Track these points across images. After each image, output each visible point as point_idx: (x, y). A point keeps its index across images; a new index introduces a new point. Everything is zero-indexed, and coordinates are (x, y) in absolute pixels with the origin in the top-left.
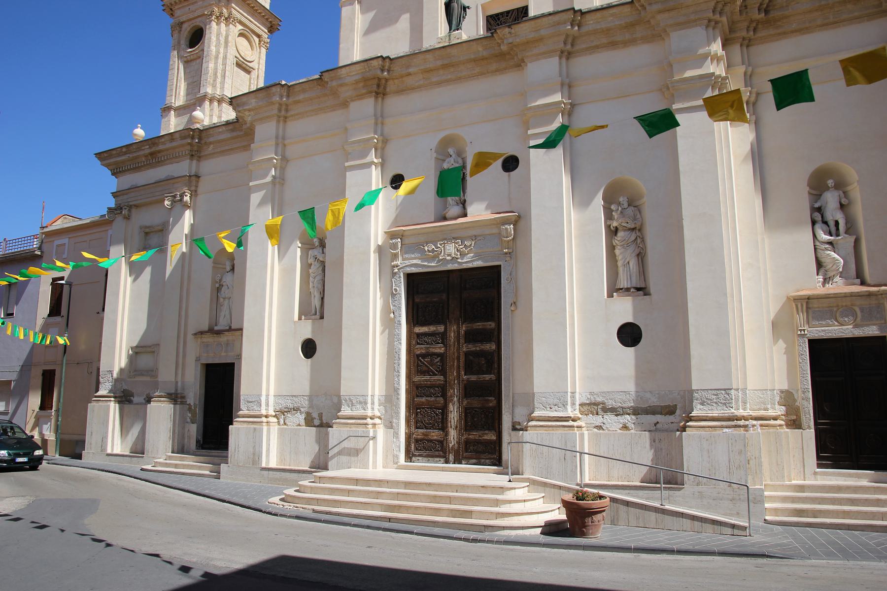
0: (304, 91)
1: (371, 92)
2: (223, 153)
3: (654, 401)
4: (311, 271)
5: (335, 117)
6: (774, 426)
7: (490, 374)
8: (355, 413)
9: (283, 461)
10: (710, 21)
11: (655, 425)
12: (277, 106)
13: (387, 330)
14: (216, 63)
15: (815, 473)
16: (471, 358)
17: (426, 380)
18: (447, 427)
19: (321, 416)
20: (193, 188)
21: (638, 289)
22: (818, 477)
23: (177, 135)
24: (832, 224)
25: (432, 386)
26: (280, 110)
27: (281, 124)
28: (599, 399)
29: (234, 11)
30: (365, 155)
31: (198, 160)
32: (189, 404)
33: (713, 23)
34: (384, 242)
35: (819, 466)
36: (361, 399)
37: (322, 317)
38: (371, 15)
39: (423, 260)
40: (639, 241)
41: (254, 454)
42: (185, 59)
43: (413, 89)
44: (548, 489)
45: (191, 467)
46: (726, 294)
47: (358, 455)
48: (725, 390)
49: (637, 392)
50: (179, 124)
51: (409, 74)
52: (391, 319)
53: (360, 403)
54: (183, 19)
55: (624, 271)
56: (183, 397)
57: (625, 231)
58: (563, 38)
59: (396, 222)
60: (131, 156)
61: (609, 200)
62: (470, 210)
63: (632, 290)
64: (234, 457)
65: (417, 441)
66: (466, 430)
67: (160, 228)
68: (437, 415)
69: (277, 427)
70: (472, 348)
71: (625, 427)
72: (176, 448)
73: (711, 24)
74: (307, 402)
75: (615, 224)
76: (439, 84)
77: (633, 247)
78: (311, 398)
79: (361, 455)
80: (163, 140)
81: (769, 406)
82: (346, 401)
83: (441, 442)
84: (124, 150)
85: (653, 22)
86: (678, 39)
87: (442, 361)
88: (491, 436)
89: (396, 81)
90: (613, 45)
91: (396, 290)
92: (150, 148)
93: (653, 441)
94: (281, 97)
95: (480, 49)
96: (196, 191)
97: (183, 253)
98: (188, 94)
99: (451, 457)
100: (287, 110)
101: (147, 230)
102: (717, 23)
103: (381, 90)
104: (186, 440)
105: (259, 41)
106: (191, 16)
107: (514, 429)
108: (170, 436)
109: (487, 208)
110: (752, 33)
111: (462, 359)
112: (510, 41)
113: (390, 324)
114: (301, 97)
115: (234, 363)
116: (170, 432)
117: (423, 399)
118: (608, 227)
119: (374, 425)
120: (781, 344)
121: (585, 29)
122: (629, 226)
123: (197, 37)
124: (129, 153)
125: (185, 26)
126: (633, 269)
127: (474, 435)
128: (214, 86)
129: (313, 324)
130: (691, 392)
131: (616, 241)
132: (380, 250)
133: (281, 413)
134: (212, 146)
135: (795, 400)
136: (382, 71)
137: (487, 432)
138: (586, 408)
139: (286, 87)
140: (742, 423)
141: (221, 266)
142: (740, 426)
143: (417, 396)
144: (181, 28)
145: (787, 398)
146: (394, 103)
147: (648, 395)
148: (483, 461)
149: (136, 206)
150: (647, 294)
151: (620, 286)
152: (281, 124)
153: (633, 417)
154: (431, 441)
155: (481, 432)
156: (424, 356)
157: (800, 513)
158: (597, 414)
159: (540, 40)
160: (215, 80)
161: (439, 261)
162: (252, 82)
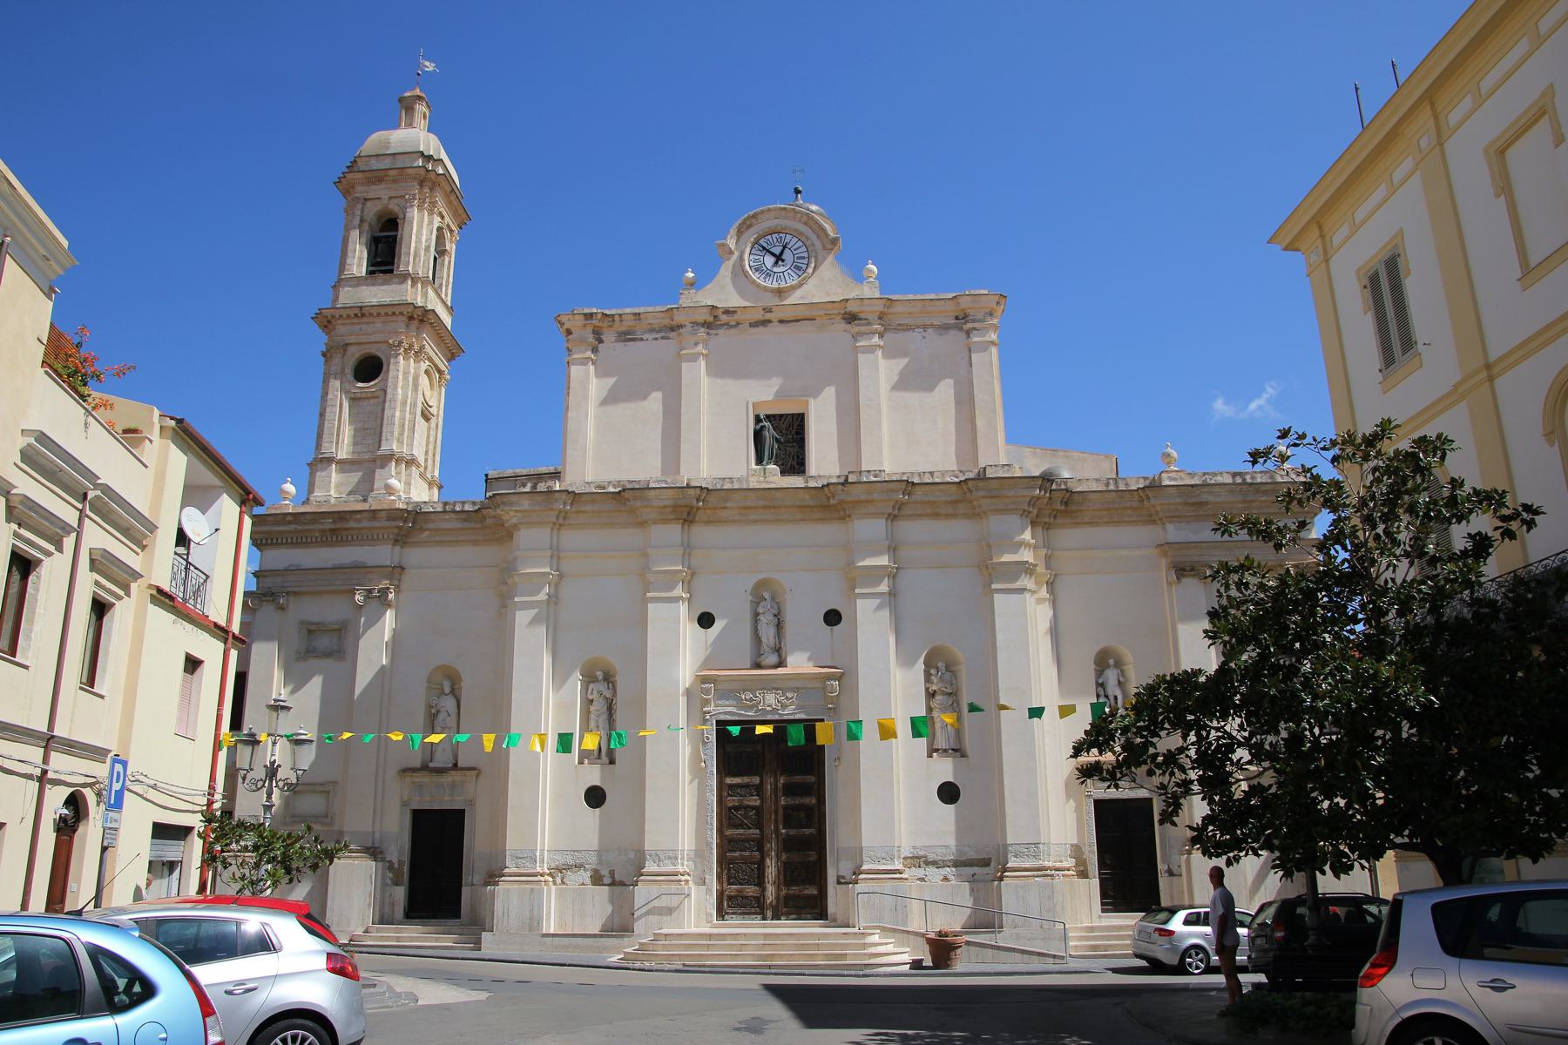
0: (593, 502)
1: (680, 519)
2: (441, 543)
3: (972, 855)
4: (592, 708)
5: (628, 537)
6: (1068, 876)
7: (809, 827)
8: (663, 869)
9: (564, 926)
10: (1024, 511)
11: (973, 876)
12: (556, 513)
13: (697, 780)
14: (403, 411)
15: (1100, 917)
16: (790, 811)
17: (739, 834)
18: (764, 882)
19: (612, 873)
20: (397, 583)
22: (1103, 920)
23: (383, 514)
24: (1112, 698)
25: (748, 840)
26: (557, 517)
27: (555, 531)
28: (921, 853)
29: (427, 346)
30: (672, 588)
31: (402, 547)
32: (390, 862)
33: (1026, 513)
34: (691, 685)
35: (1103, 911)
36: (671, 854)
37: (612, 762)
38: (611, 381)
39: (739, 708)
40: (955, 705)
41: (531, 919)
42: (353, 396)
43: (725, 522)
44: (897, 935)
45: (417, 939)
46: (1035, 760)
47: (671, 914)
48: (1034, 844)
49: (957, 846)
50: (342, 484)
51: (725, 508)
52: (701, 768)
53: (670, 858)
54: (352, 339)
55: (942, 732)
56: (381, 852)
57: (943, 695)
58: (892, 504)
59: (706, 664)
60: (299, 528)
61: (929, 664)
62: (790, 660)
63: (950, 751)
64: (502, 923)
65: (730, 898)
66: (785, 885)
67: (336, 627)
68: (752, 870)
69: (553, 887)
70: (791, 801)
71: (946, 879)
72: (377, 917)
73: (1025, 513)
74: (594, 858)
75: (934, 688)
76: (755, 522)
78: (599, 853)
79: (675, 915)
80: (359, 516)
81: (1063, 859)
82: (651, 855)
83: (757, 899)
84: (289, 518)
85: (975, 503)
86: (998, 524)
87: (757, 814)
88: (813, 891)
89: (708, 511)
90: (936, 515)
91: (708, 738)
92: (334, 522)
93: (972, 890)
94: (565, 504)
95: (807, 497)
96: (398, 586)
97: (383, 666)
98: (355, 444)
99: (769, 914)
100: (565, 518)
101: (313, 628)
102: (1029, 512)
103: (691, 518)
104: (386, 908)
105: (440, 378)
106: (364, 339)
107: (839, 883)
108: (370, 902)
109: (810, 659)
110: (1052, 520)
111: (781, 812)
112: (842, 498)
113: (698, 772)
114: (589, 508)
115: (464, 810)
116: (370, 898)
117: (737, 854)
118: (927, 689)
119: (687, 881)
120: (1072, 803)
121: (913, 498)
122: (948, 691)
123: (370, 368)
124: (296, 524)
125: (351, 349)
127: (794, 890)
128: (400, 442)
129: (602, 770)
130: (1006, 846)
132: (688, 692)
133: (559, 870)
134: (427, 533)
135: (1083, 854)
136: (698, 500)
137: (807, 887)
138: (909, 861)
139: (572, 495)
140: (1048, 872)
141: (433, 686)
142: (1048, 875)
143: (730, 851)
144: (345, 350)
145: (1077, 851)
146: (702, 534)
147: (967, 849)
148: (803, 916)
149: (295, 593)
150: (963, 755)
152: (555, 531)
153: (954, 869)
154: (746, 898)
155: (801, 887)
156: (737, 808)
157: (1095, 948)
158: (919, 867)
159: (871, 501)
160: (401, 434)
161: (758, 710)
162: (432, 433)
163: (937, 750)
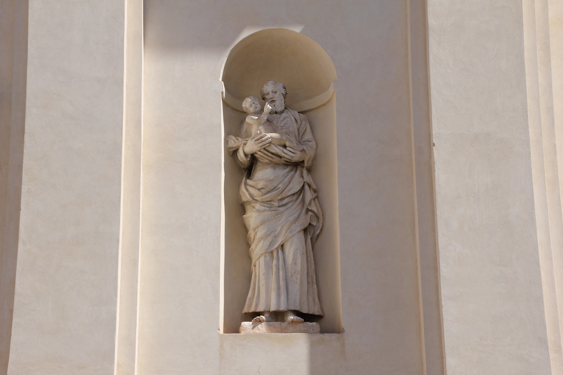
21: (308, 317)
40: (309, 195)
46: (543, 341)
55: (268, 267)
57: (275, 165)
63: (291, 317)
75: (251, 147)
77: (294, 209)
118: (232, 154)
122: (288, 154)
126: (294, 260)
131: (252, 190)
151: (250, 306)
163: (252, 316)
